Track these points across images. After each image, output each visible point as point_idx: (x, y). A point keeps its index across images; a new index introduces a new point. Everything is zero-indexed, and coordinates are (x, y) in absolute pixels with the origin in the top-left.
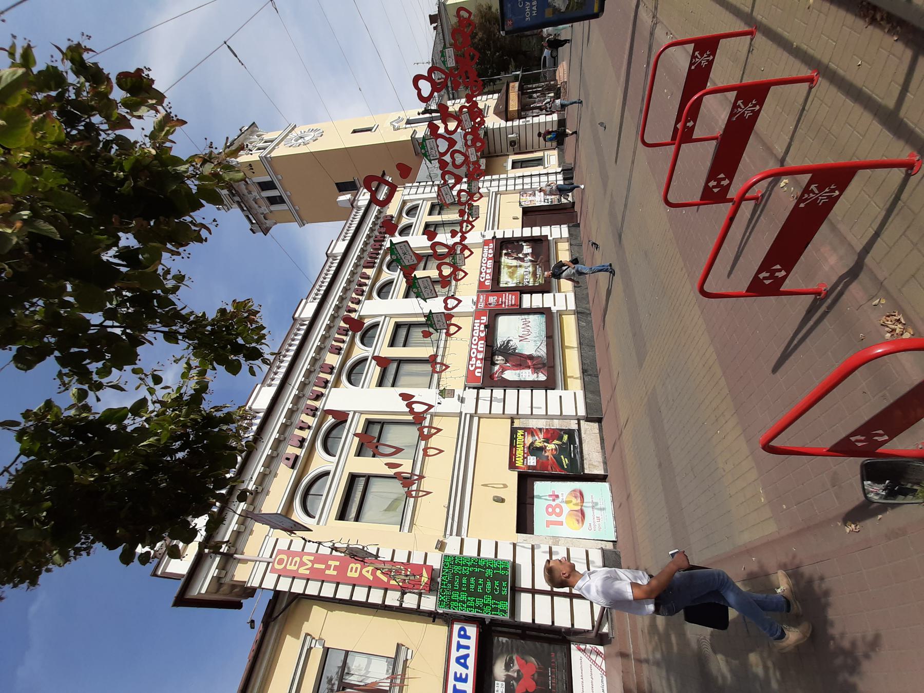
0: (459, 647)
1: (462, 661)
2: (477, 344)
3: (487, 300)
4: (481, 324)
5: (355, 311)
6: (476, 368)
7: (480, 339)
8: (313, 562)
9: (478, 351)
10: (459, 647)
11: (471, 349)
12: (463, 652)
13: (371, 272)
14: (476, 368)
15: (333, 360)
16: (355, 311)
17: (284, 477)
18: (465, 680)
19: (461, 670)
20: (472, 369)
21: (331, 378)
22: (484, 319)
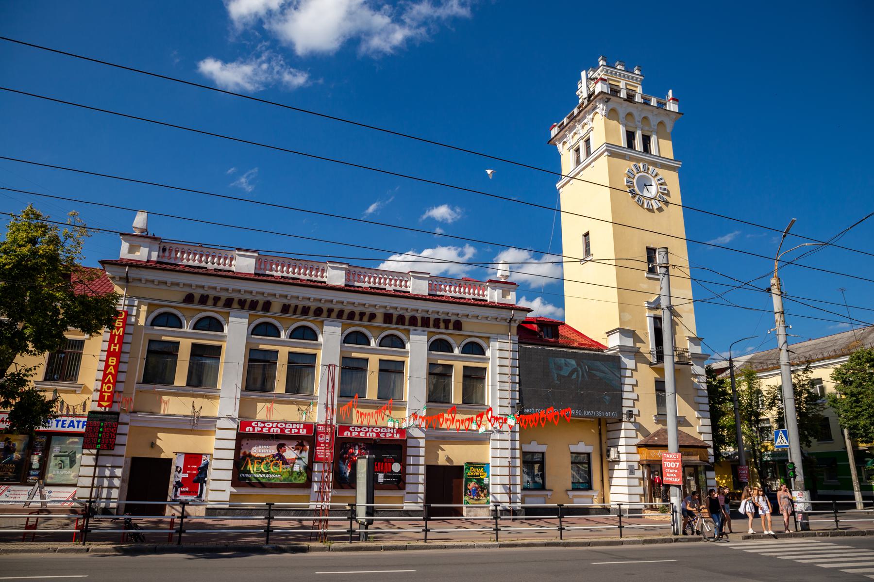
0: (79, 422)
1: (72, 424)
2: (277, 427)
3: (326, 433)
4: (299, 429)
6: (254, 428)
7: (282, 430)
8: (119, 335)
9: (270, 428)
10: (79, 422)
11: (273, 423)
12: (76, 424)
13: (379, 322)
14: (254, 428)
15: (276, 308)
18: (62, 426)
19: (67, 423)
20: (253, 424)
22: (303, 432)
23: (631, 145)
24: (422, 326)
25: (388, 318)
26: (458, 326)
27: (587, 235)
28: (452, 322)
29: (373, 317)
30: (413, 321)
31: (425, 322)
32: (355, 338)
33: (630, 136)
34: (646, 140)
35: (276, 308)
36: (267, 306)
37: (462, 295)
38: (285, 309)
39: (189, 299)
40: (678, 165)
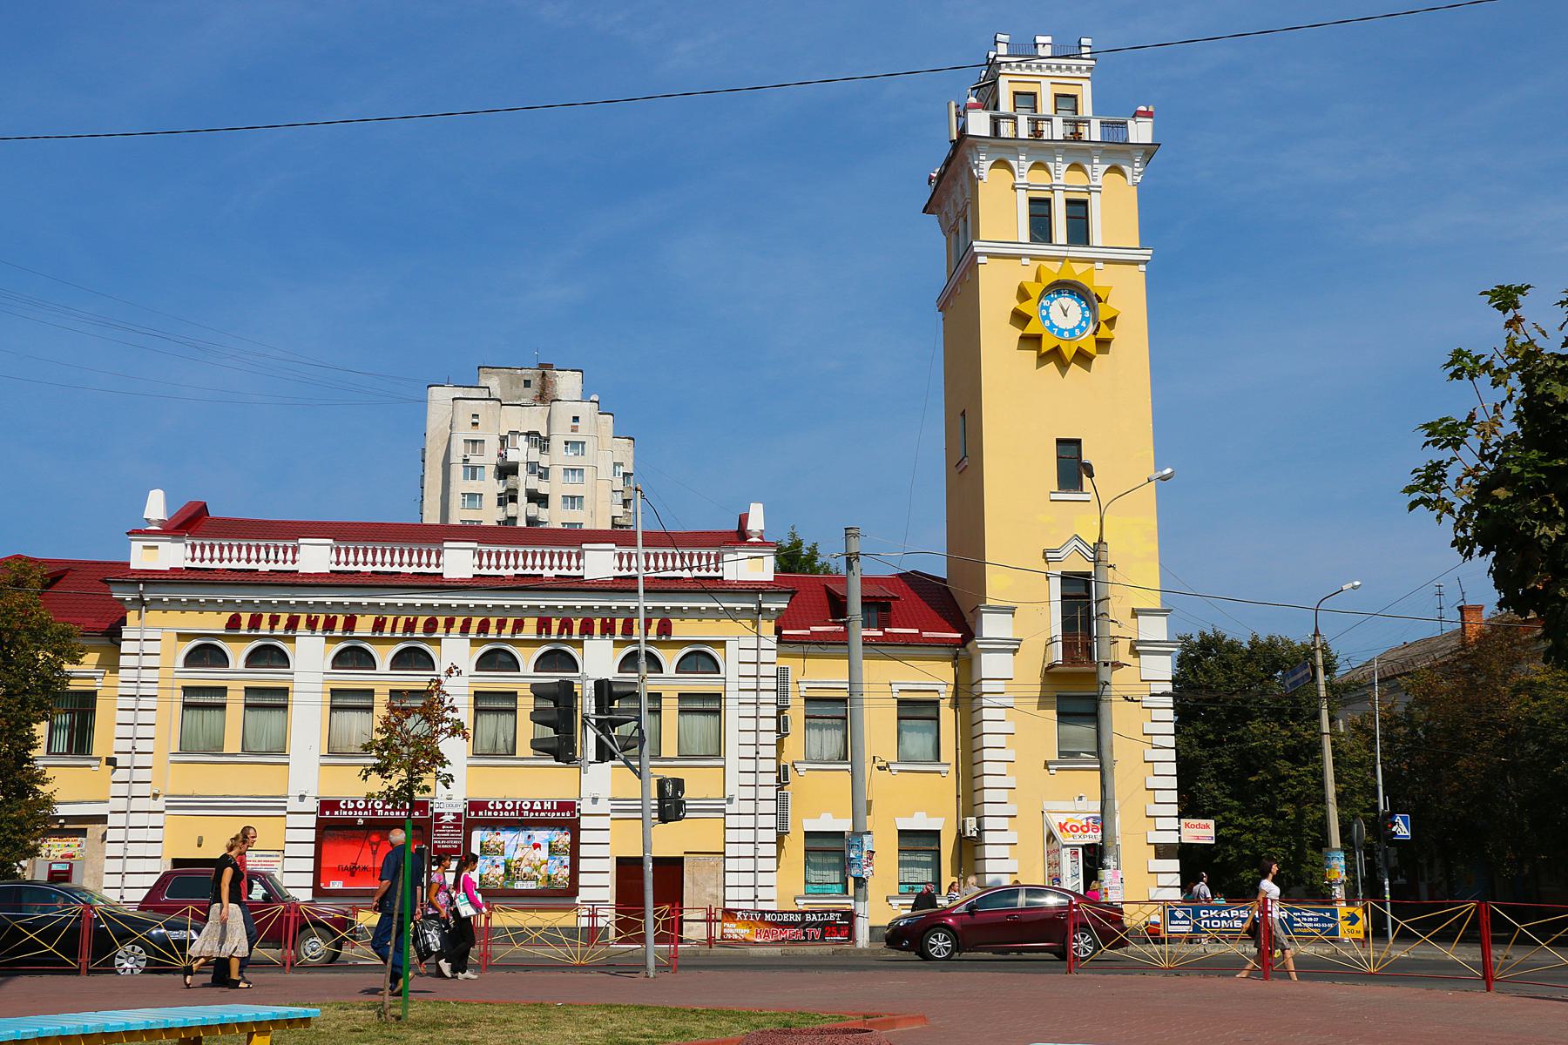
5: (448, 632)
13: (530, 630)
15: (364, 626)
16: (448, 632)
17: (215, 622)
21: (338, 632)
23: (1041, 227)
24: (603, 634)
25: (544, 624)
26: (665, 628)
27: (963, 414)
28: (655, 622)
29: (519, 625)
30: (587, 629)
31: (608, 629)
32: (496, 660)
33: (1040, 211)
34: (1078, 211)
35: (364, 626)
36: (350, 624)
37: (678, 574)
38: (379, 625)
39: (234, 623)
40: (1146, 254)
